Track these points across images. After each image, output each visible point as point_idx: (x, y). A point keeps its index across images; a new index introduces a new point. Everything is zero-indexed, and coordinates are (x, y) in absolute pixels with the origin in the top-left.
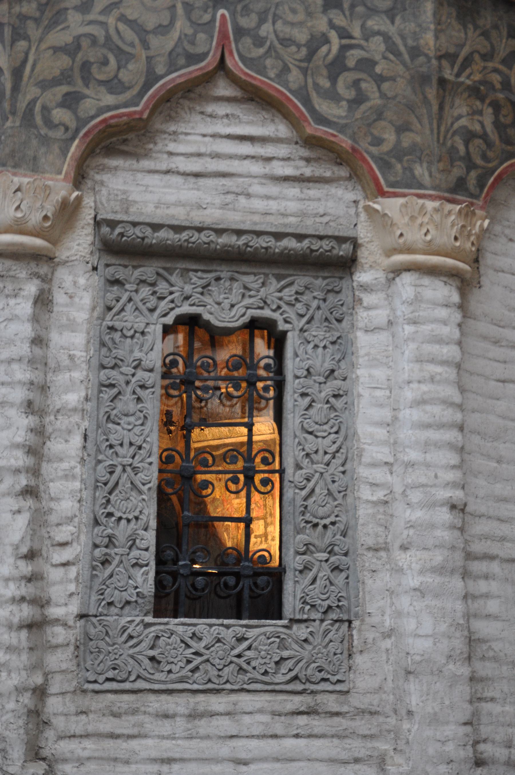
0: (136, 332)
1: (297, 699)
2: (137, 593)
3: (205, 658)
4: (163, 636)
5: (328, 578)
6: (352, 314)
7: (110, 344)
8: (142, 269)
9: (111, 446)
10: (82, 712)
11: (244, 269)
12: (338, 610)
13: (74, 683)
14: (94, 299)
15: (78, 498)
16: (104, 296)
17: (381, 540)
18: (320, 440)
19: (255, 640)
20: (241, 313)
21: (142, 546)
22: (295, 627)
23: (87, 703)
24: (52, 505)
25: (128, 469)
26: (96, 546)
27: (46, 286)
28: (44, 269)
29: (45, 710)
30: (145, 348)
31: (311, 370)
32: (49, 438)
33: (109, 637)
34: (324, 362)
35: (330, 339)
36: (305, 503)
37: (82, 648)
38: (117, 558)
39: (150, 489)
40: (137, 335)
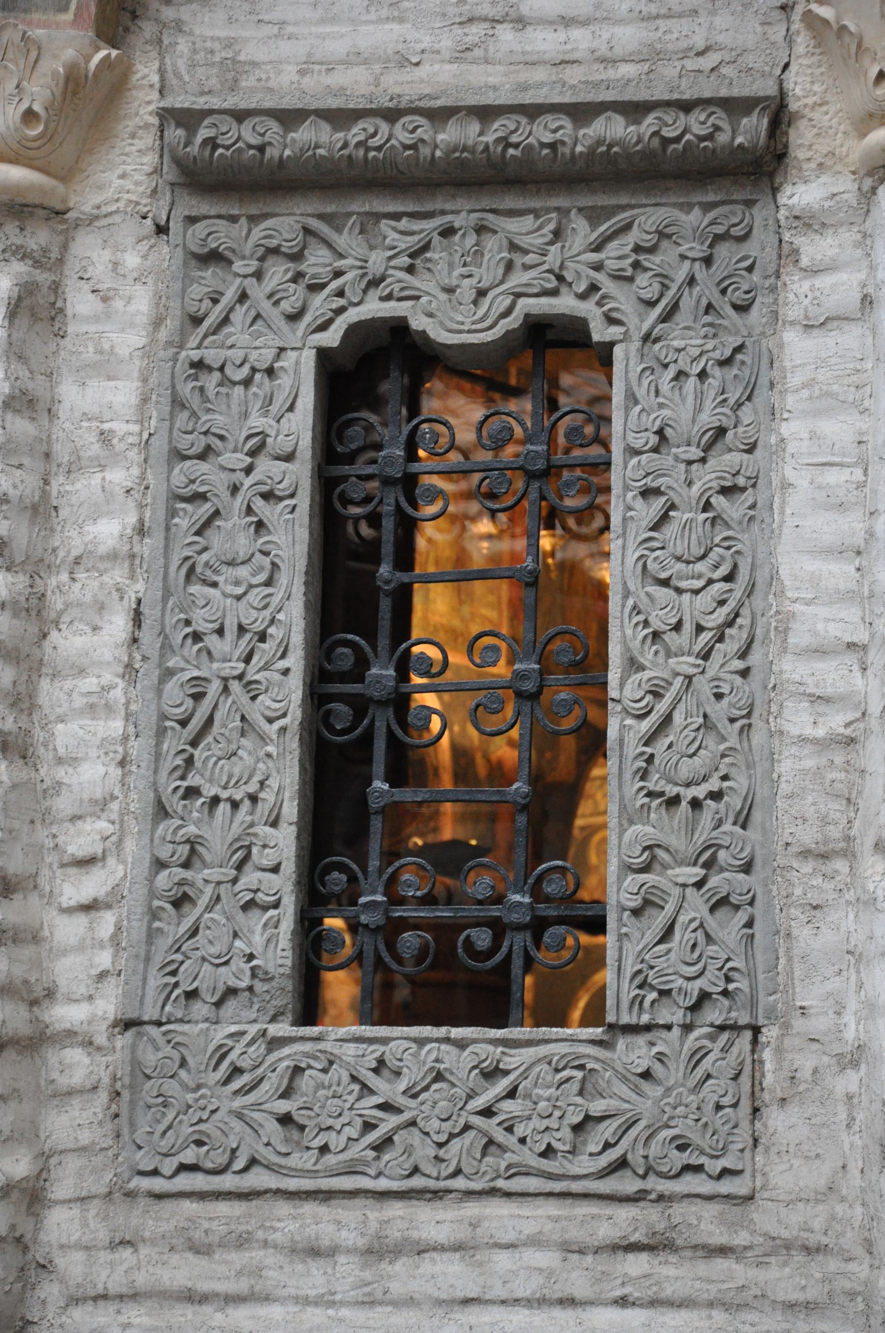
0: (254, 370)
1: (624, 1213)
2: (253, 969)
3: (407, 1116)
4: (310, 1067)
5: (701, 925)
6: (773, 289)
7: (195, 402)
8: (269, 223)
9: (197, 637)
10: (125, 1243)
11: (510, 202)
12: (726, 1002)
13: (108, 1176)
14: (158, 298)
15: (119, 757)
16: (184, 291)
17: (835, 832)
18: (686, 597)
19: (524, 1075)
20: (502, 309)
21: (265, 862)
22: (621, 1043)
23: (134, 1222)
24: (61, 773)
25: (235, 686)
26: (160, 865)
27: (43, 278)
28: (39, 237)
29: (43, 1237)
30: (274, 408)
31: (668, 432)
32: (57, 623)
33: (189, 1071)
34: (699, 409)
35: (717, 355)
36: (649, 750)
37: (126, 1095)
38: (209, 890)
39: (283, 730)
40: (258, 376)
